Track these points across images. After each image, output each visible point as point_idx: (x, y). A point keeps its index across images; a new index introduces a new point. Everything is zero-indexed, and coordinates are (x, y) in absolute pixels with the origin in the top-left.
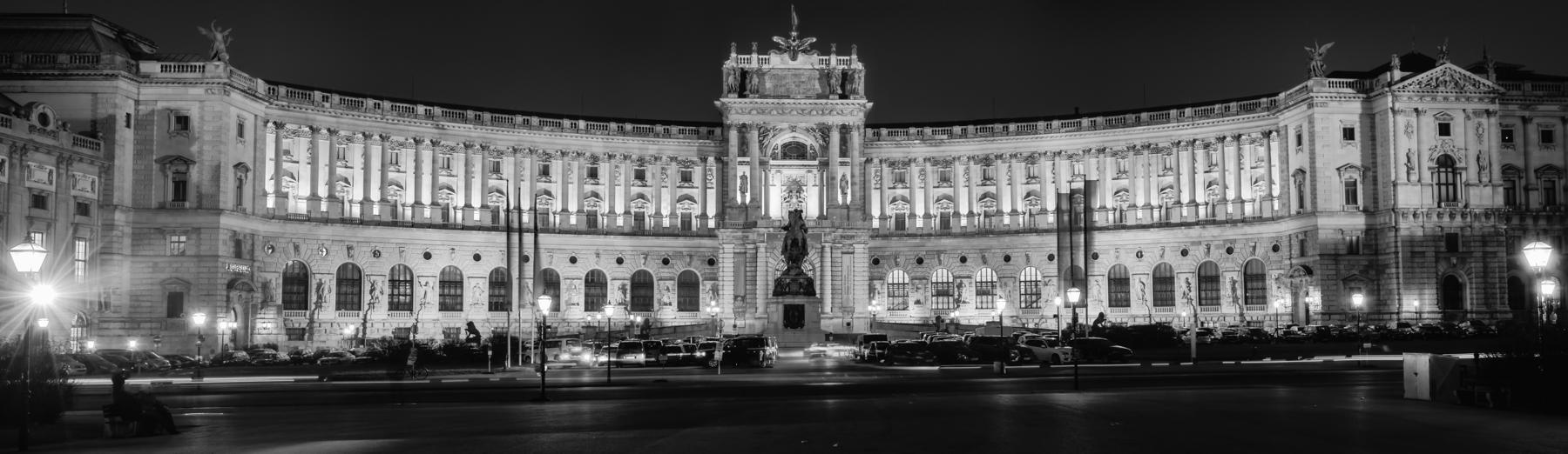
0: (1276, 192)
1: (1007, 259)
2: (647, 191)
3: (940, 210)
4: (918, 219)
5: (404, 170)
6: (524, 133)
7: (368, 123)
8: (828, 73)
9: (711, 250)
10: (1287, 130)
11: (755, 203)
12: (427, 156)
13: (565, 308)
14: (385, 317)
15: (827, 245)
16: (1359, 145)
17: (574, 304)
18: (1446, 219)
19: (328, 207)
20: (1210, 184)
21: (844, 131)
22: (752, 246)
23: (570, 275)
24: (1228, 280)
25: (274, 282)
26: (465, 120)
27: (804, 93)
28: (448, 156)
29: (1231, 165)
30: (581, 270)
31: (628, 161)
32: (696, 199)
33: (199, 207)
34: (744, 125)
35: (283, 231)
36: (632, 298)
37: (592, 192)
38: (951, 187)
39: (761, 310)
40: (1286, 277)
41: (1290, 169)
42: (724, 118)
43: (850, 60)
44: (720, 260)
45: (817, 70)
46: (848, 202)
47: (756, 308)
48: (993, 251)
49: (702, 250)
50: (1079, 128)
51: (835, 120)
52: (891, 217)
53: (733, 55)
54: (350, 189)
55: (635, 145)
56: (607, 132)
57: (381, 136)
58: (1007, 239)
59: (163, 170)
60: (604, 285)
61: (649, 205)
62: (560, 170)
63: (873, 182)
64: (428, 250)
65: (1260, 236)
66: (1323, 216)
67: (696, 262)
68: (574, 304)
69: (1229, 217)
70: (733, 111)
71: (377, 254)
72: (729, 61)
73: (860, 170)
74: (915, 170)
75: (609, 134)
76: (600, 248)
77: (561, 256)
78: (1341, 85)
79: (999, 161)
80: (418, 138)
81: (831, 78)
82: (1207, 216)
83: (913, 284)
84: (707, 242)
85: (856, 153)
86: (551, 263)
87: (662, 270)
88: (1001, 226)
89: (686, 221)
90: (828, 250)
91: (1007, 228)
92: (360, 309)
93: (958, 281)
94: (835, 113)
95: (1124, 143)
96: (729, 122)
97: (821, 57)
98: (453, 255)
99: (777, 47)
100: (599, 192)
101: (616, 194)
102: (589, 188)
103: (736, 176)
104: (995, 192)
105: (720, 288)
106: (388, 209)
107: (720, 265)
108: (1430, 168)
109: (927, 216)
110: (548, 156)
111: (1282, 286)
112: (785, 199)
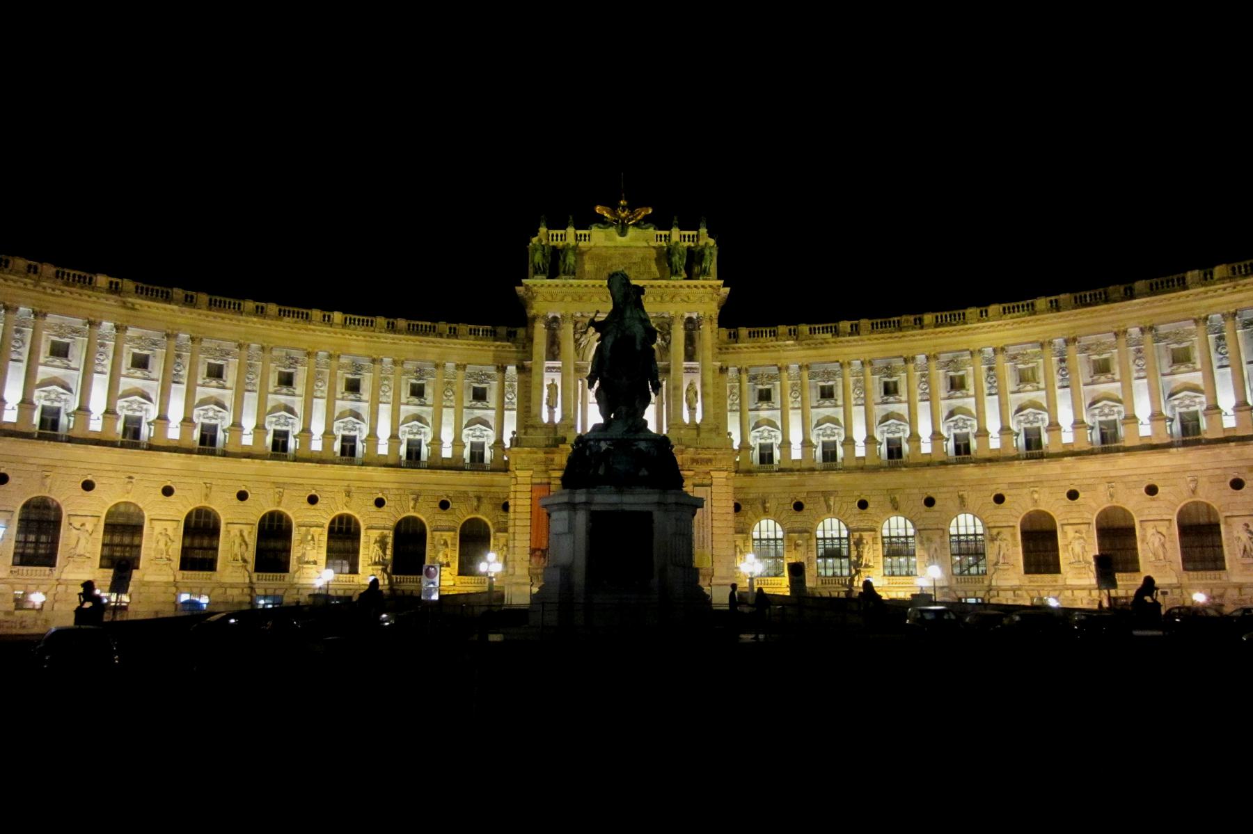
1: (930, 502)
2: (427, 412)
6: (254, 323)
7: (10, 290)
8: (669, 249)
11: (568, 421)
13: (296, 568)
17: (308, 562)
21: (691, 326)
23: (307, 520)
28: (145, 352)
30: (324, 515)
31: (398, 368)
34: (555, 319)
37: (351, 410)
42: (527, 311)
43: (698, 236)
45: (654, 247)
46: (698, 420)
48: (907, 491)
49: (493, 489)
50: (1033, 311)
53: (543, 230)
56: (372, 329)
58: (929, 474)
67: (486, 506)
68: (308, 562)
70: (540, 298)
72: (535, 240)
75: (374, 331)
79: (911, 366)
81: (673, 255)
83: (789, 539)
84: (499, 478)
86: (279, 503)
87: (437, 517)
89: (477, 455)
91: (927, 459)
93: (857, 535)
94: (679, 299)
96: (533, 312)
97: (659, 232)
99: (601, 221)
100: (360, 411)
103: (542, 385)
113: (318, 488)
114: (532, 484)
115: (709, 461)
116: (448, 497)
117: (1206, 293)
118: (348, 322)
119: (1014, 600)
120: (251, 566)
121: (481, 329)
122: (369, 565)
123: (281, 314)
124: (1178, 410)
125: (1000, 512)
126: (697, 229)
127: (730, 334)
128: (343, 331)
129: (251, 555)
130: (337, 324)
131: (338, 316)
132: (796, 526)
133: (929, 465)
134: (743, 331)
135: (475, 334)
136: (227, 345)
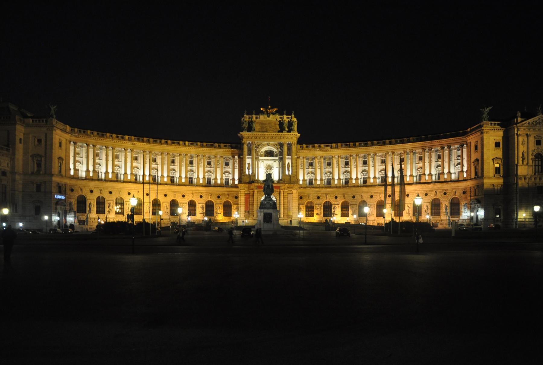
0: (465, 169)
2: (212, 169)
3: (327, 177)
4: (318, 181)
5: (121, 161)
6: (165, 146)
7: (107, 143)
9: (236, 193)
10: (471, 144)
12: (129, 155)
14: (114, 216)
15: (281, 190)
16: (502, 149)
18: (538, 180)
19: (93, 175)
20: (438, 166)
21: (289, 145)
22: (252, 191)
24: (444, 206)
25: (73, 202)
26: (143, 141)
27: (273, 130)
28: (137, 155)
29: (446, 159)
30: (186, 200)
32: (231, 172)
33: (45, 173)
35: (76, 183)
36: (206, 211)
38: (331, 168)
39: (255, 216)
40: (469, 204)
41: (472, 160)
43: (291, 117)
44: (239, 196)
45: (278, 121)
46: (290, 173)
47: (253, 216)
49: (233, 192)
50: (385, 144)
51: (285, 141)
52: (307, 180)
53: (245, 115)
54: (101, 168)
55: (206, 151)
56: (196, 146)
57: (112, 148)
58: (354, 189)
59: (33, 160)
60: (195, 206)
61: (212, 175)
62: (179, 161)
63: (300, 166)
64: (129, 192)
65: (458, 187)
66: (486, 179)
67: (230, 197)
69: (445, 180)
71: (111, 193)
73: (295, 161)
74: (317, 161)
75: (197, 147)
76: (194, 191)
77: (179, 194)
78: (495, 124)
80: (125, 148)
81: (284, 124)
82: (435, 180)
84: (234, 189)
85: (294, 154)
86: (175, 197)
88: (351, 183)
90: (282, 192)
91: (354, 185)
92: (105, 214)
94: (285, 138)
95: (403, 150)
97: (280, 116)
98: (139, 194)
99: (262, 113)
100: (193, 170)
101: (200, 171)
102: (189, 168)
103: (246, 163)
104: (349, 170)
105: (239, 207)
106: (115, 175)
107: (239, 198)
108: (531, 159)
109: (339, 179)
110: (174, 156)
111: (466, 208)
112: (265, 172)
113: (184, 193)
114: (245, 193)
115: (292, 187)
116: (220, 195)
117: (425, 143)
119: (373, 224)
120: (169, 214)
122: (199, 214)
123: (172, 143)
124: (418, 173)
125: (372, 200)
126: (291, 115)
127: (301, 146)
128: (189, 147)
129: (169, 211)
130: (187, 145)
131: (187, 143)
132: (318, 203)
133: (354, 186)
134: (305, 146)
136: (157, 152)
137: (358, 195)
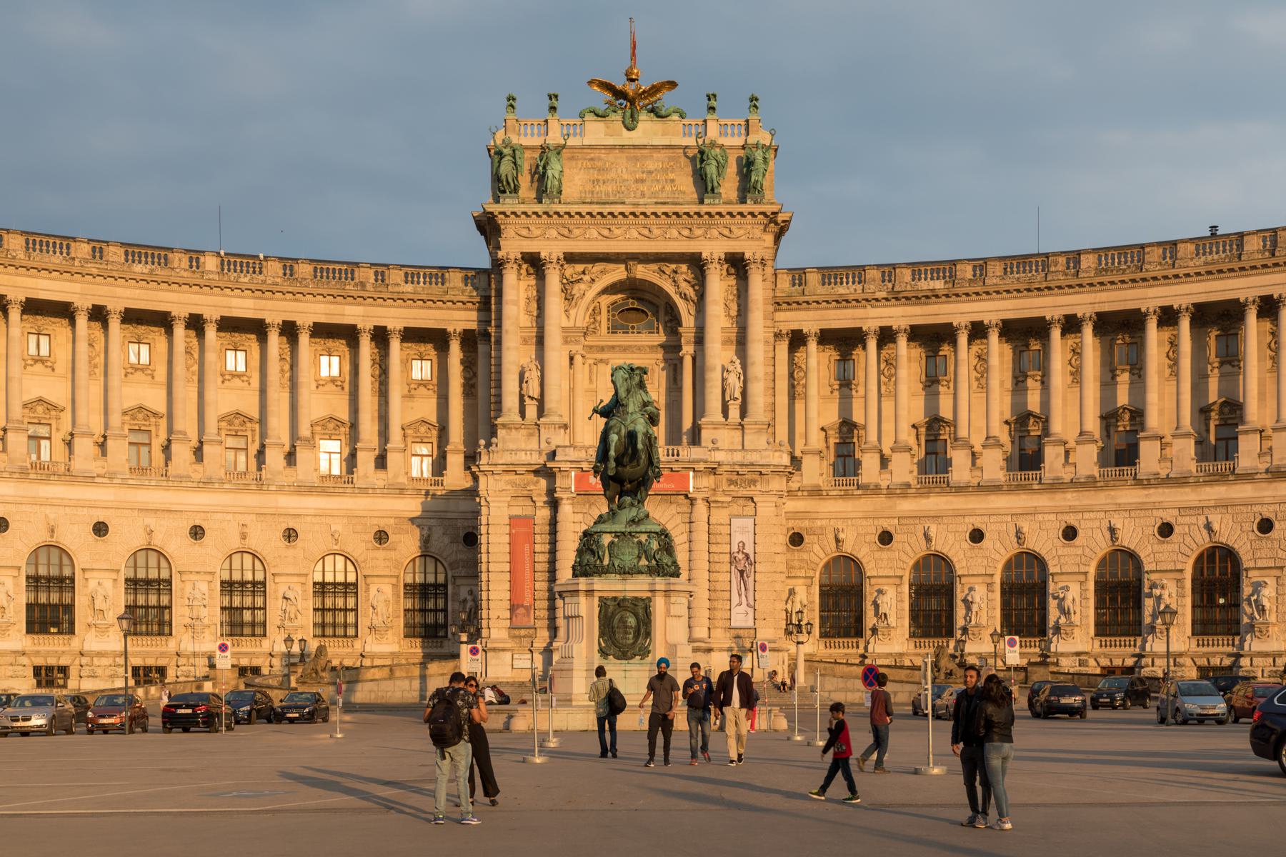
48: (1040, 517)
56: (261, 277)
118: (226, 267)
121: (422, 274)
135: (412, 283)
137: (1090, 524)
